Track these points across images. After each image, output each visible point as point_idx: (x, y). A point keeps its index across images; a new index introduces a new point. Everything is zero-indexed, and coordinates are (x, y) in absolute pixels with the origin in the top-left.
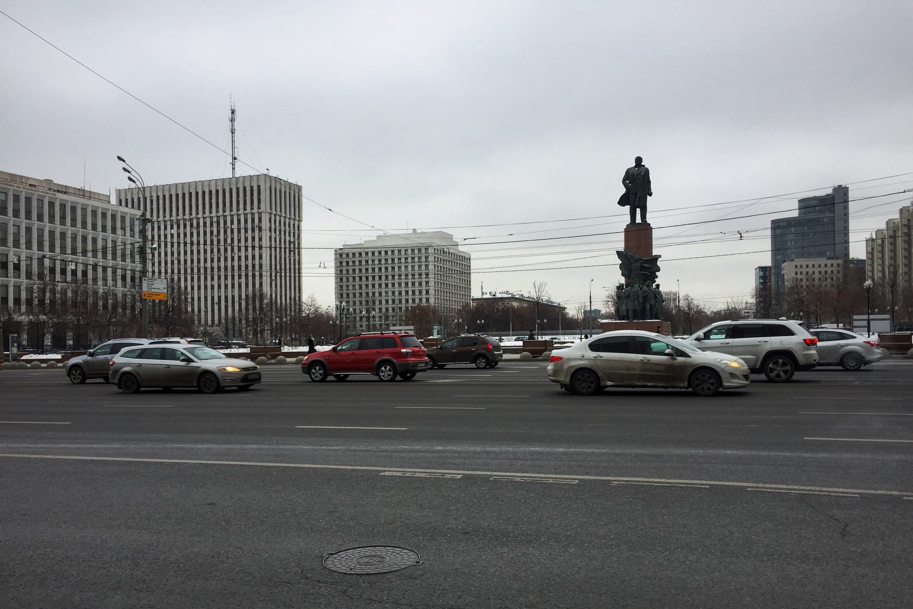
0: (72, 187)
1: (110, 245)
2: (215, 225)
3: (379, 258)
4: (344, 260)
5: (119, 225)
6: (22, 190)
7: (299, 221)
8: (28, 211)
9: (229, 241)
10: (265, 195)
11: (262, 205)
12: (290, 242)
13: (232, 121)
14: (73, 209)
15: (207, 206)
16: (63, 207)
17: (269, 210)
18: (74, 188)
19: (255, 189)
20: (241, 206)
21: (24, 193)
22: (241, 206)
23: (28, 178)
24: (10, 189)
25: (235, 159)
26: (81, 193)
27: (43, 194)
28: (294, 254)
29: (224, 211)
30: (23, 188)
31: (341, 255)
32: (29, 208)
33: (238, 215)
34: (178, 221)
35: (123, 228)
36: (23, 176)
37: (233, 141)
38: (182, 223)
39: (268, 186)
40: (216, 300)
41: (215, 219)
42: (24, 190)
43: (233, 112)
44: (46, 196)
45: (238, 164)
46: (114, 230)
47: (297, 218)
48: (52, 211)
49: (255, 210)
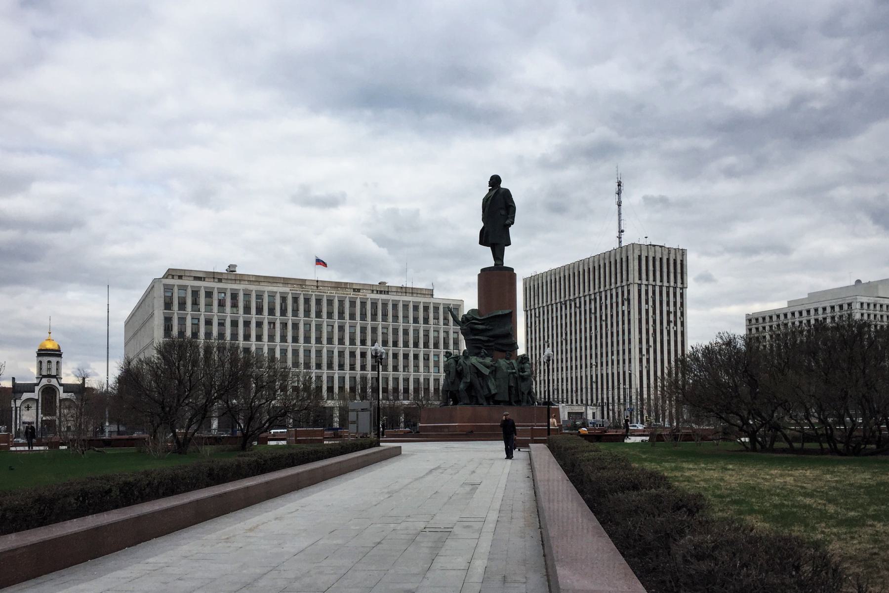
0: (394, 287)
1: (442, 335)
2: (593, 303)
3: (793, 320)
4: (754, 326)
5: (431, 315)
6: (334, 295)
7: (682, 289)
8: (341, 312)
9: (604, 318)
10: (634, 265)
11: (631, 276)
12: (669, 313)
13: (618, 194)
14: (385, 305)
15: (586, 284)
16: (374, 305)
17: (637, 281)
18: (396, 287)
19: (624, 260)
20: (613, 280)
21: (336, 298)
22: (613, 280)
23: (352, 283)
24: (324, 295)
25: (622, 231)
26: (404, 290)
27: (354, 296)
28: (676, 324)
29: (600, 288)
30: (336, 293)
31: (750, 320)
32: (343, 311)
33: (611, 290)
34: (566, 301)
35: (436, 318)
36: (347, 283)
37: (620, 214)
38: (568, 303)
39: (636, 256)
40: (594, 379)
41: (593, 297)
42: (337, 295)
43: (619, 185)
44: (346, 297)
45: (624, 236)
46: (426, 321)
47: (679, 285)
48: (364, 310)
49: (624, 283)
